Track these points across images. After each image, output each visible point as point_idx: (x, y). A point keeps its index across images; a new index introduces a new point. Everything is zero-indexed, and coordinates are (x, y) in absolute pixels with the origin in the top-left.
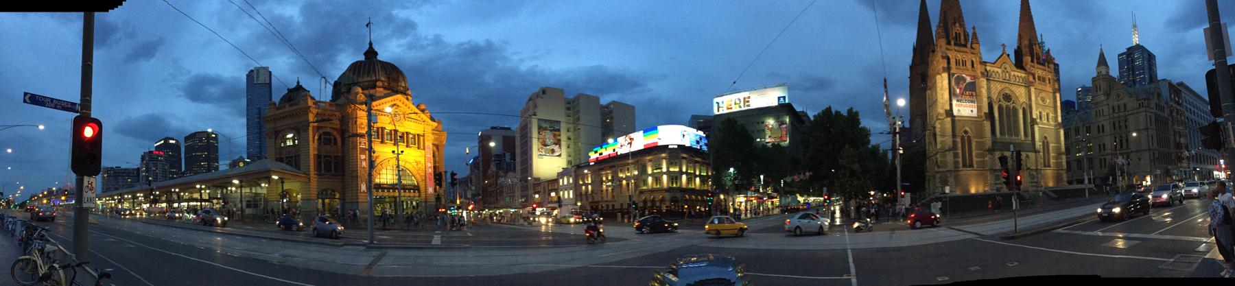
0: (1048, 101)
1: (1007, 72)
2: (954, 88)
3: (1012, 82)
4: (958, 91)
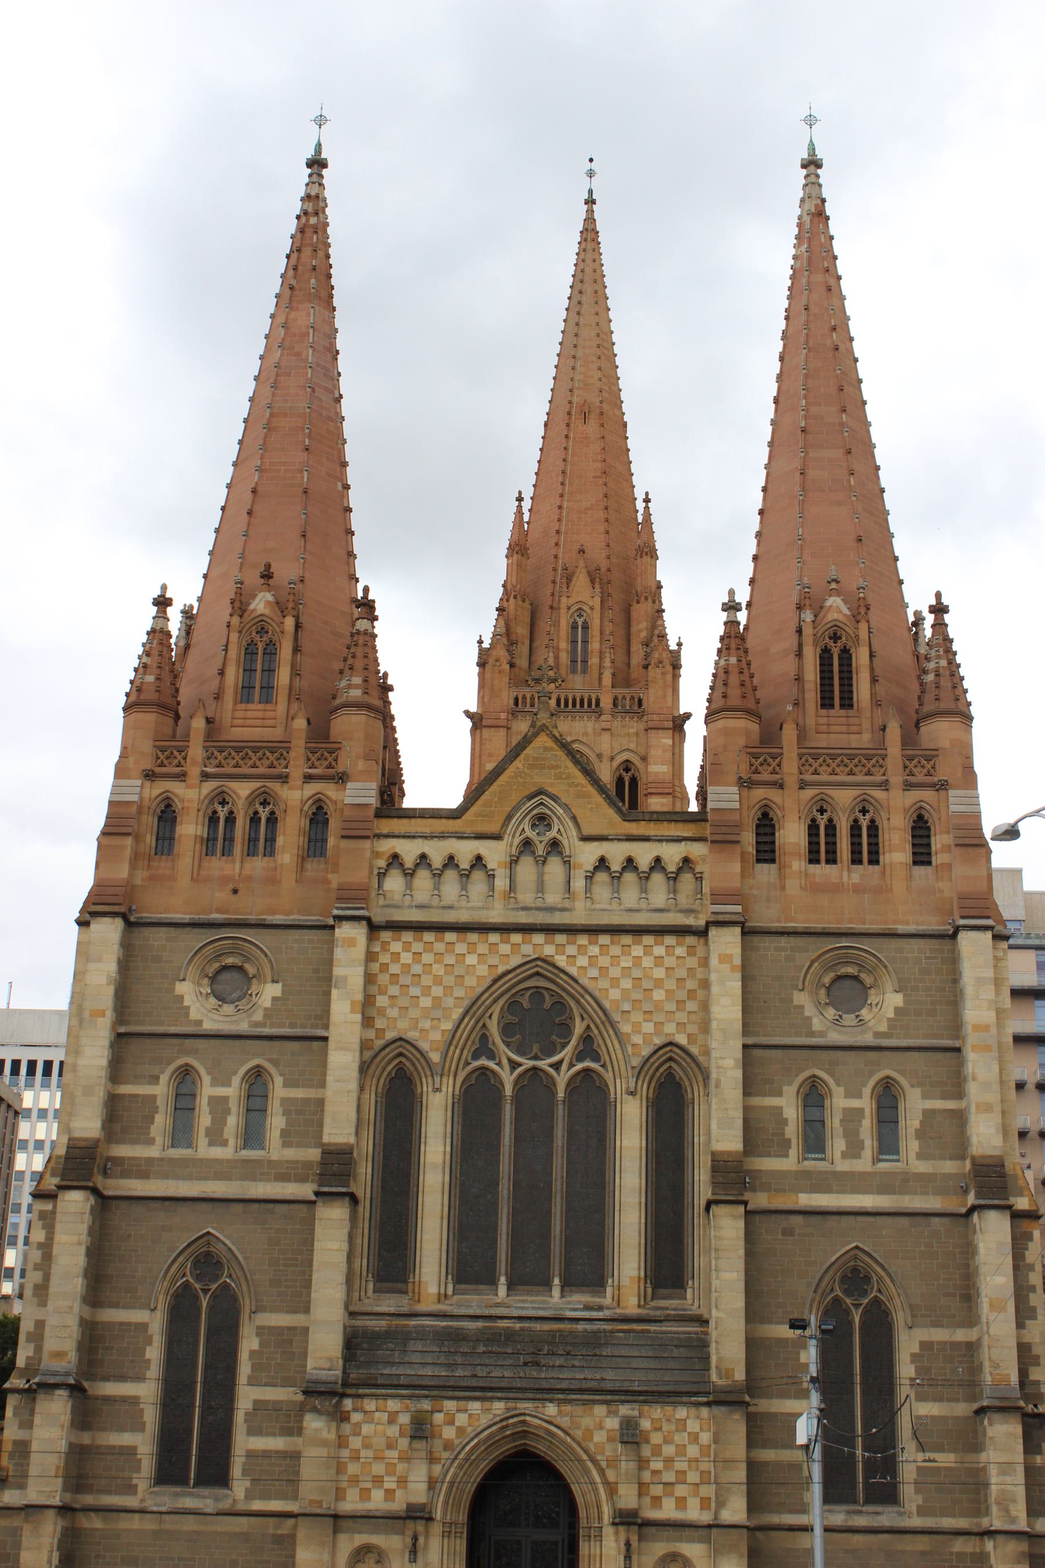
0: (896, 1000)
1: (555, 845)
3: (579, 915)
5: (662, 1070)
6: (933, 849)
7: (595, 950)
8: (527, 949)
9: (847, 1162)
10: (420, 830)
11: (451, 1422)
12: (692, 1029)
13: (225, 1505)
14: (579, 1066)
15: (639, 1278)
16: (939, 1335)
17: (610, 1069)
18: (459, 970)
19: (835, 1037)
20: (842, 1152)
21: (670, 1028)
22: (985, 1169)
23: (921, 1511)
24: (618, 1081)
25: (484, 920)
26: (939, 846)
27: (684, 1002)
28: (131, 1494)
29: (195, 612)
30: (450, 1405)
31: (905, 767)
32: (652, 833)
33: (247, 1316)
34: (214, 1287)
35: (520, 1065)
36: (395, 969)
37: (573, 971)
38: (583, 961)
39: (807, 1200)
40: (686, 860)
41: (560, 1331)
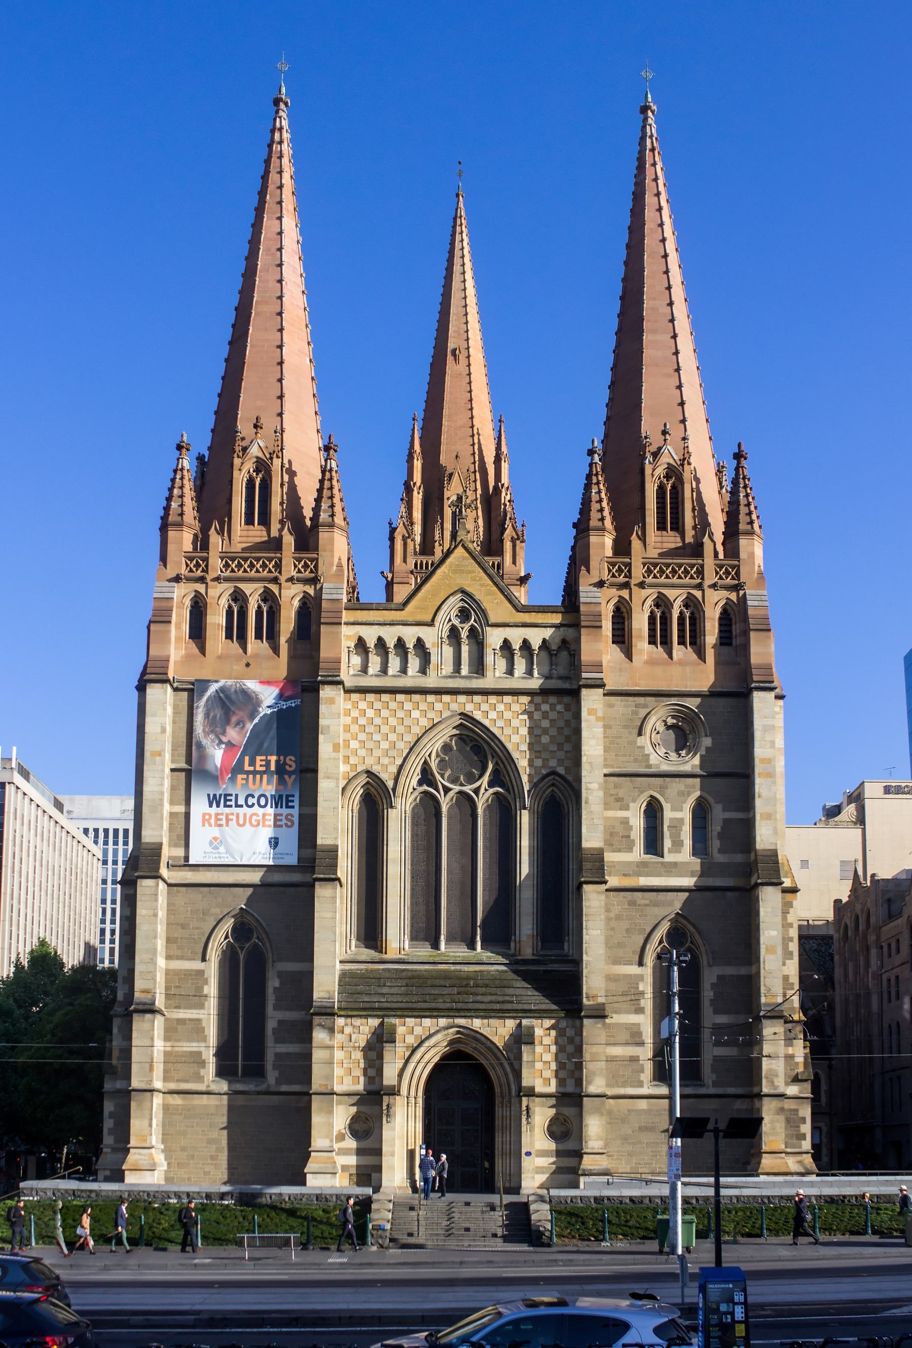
2: (200, 746)
4: (217, 755)
5: (547, 792)
6: (734, 633)
7: (500, 707)
8: (454, 707)
9: (672, 855)
10: (376, 619)
11: (412, 1032)
12: (568, 763)
13: (263, 1087)
14: (491, 791)
15: (533, 936)
16: (730, 971)
17: (512, 792)
18: (407, 722)
19: (665, 767)
20: (669, 848)
21: (553, 763)
22: (765, 858)
23: (715, 1084)
24: (518, 800)
25: (423, 686)
26: (738, 631)
27: (563, 744)
28: (200, 1082)
29: (206, 460)
30: (410, 1021)
31: (717, 573)
32: (540, 621)
33: (270, 964)
34: (247, 945)
35: (450, 790)
36: (362, 721)
37: (486, 722)
38: (493, 715)
39: (644, 881)
40: (564, 641)
41: (481, 971)
